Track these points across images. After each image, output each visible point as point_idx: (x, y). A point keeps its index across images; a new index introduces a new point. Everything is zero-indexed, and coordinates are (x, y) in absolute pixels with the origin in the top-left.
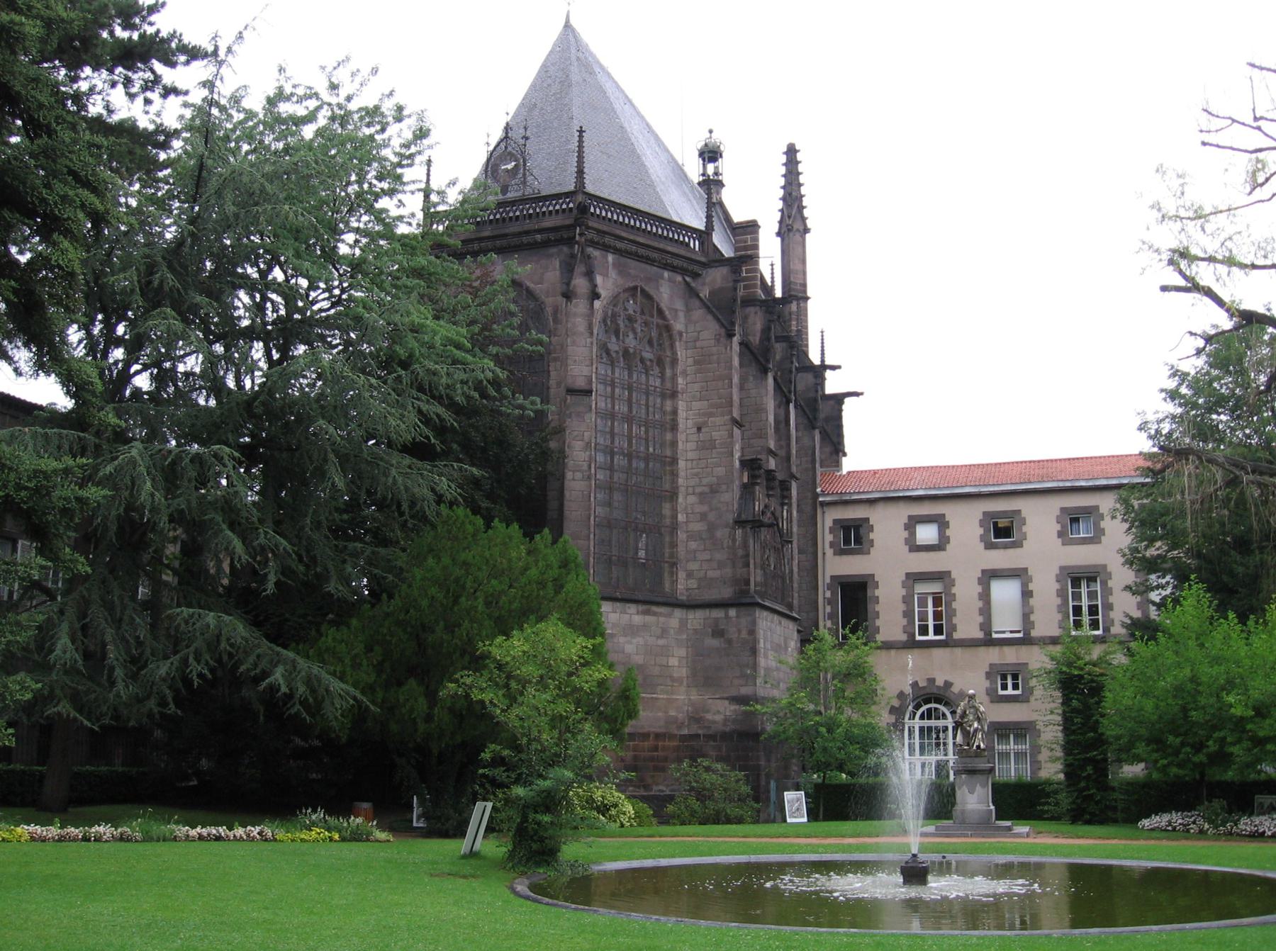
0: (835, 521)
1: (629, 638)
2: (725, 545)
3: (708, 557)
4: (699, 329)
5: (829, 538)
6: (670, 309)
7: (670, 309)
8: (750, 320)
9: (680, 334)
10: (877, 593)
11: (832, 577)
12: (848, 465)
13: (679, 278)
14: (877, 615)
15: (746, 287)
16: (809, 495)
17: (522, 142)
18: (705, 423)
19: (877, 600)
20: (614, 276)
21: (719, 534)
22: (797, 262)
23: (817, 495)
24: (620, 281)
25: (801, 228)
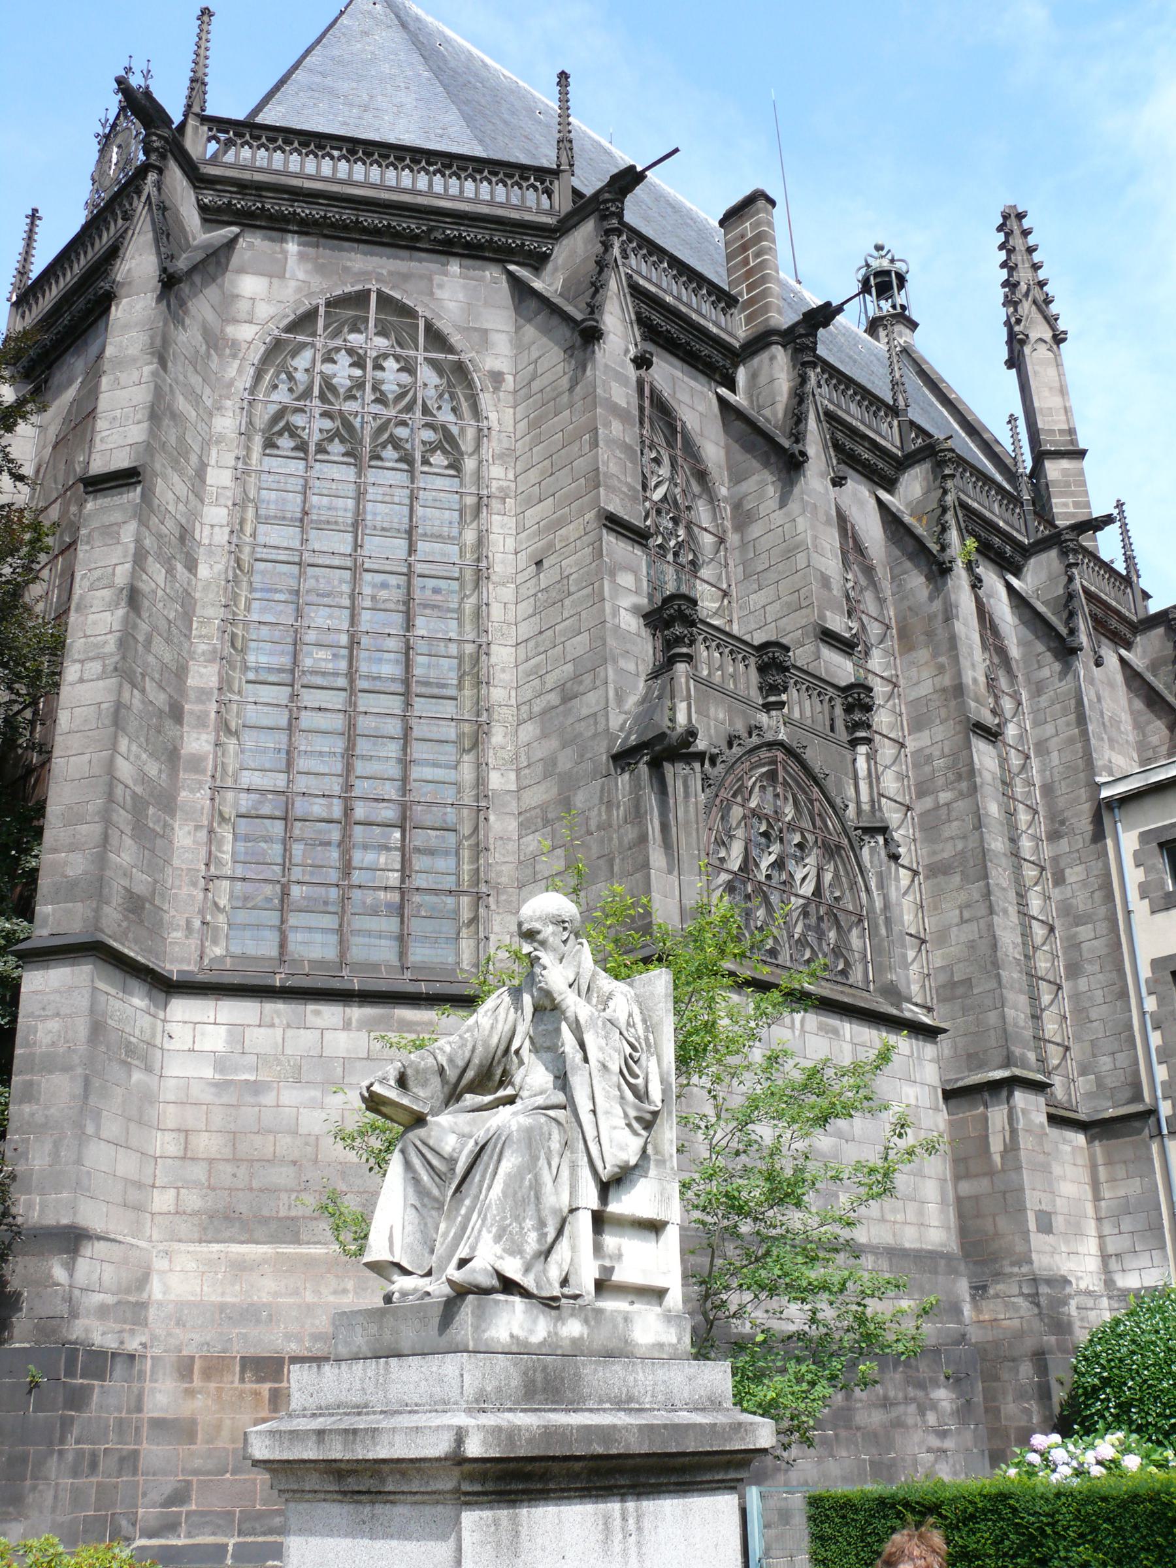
0: (1144, 837)
2: (593, 824)
5: (1134, 876)
6: (465, 330)
7: (465, 330)
8: (762, 379)
9: (497, 378)
11: (1156, 963)
15: (749, 319)
16: (1083, 793)
20: (301, 275)
22: (1046, 393)
24: (317, 283)
25: (1048, 335)
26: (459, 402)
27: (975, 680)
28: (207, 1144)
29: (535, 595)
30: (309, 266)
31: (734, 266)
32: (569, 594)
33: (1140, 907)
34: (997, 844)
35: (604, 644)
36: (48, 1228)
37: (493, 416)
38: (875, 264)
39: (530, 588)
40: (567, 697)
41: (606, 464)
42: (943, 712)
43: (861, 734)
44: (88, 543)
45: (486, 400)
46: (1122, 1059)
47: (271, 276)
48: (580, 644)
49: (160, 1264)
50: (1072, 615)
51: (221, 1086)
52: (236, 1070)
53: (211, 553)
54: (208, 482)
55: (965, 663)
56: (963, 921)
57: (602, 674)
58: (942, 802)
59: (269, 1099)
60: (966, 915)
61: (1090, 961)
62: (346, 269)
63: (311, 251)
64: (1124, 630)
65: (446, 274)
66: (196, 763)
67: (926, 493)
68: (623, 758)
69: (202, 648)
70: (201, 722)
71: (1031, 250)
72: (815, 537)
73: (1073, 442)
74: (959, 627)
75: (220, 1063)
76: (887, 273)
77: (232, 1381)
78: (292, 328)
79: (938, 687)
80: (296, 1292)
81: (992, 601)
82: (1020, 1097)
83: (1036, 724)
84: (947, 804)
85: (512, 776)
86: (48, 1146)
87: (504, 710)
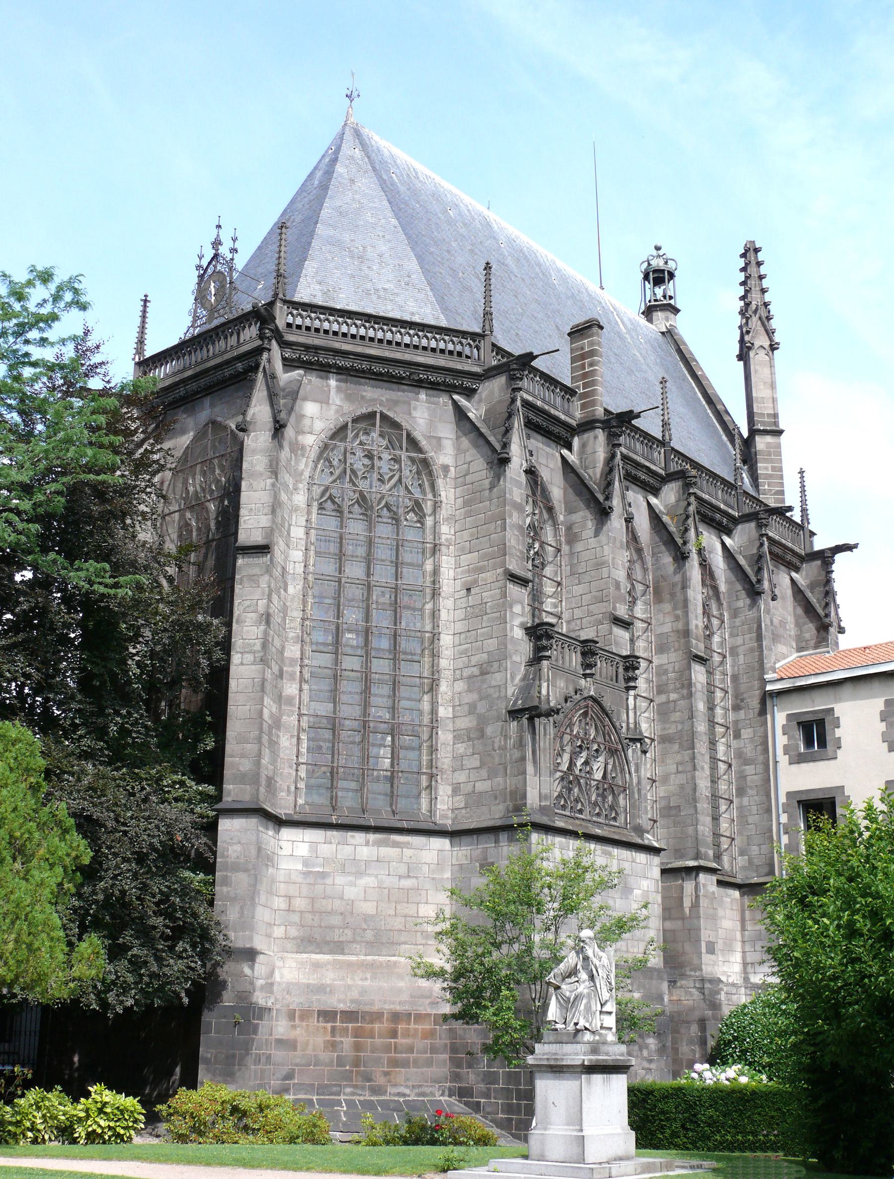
0: (790, 717)
2: (496, 746)
4: (469, 459)
5: (782, 740)
6: (429, 438)
7: (429, 438)
8: (589, 450)
9: (446, 469)
11: (789, 794)
12: (845, 642)
15: (583, 406)
16: (756, 684)
17: (229, 256)
18: (476, 581)
20: (338, 402)
21: (489, 731)
22: (762, 387)
23: (765, 682)
25: (766, 344)
26: (423, 481)
27: (697, 626)
28: (300, 903)
29: (466, 608)
30: (343, 396)
31: (576, 367)
32: (486, 614)
34: (701, 727)
35: (506, 648)
36: (239, 948)
37: (443, 494)
38: (654, 263)
39: (462, 603)
40: (484, 673)
41: (509, 541)
42: (676, 644)
43: (632, 684)
44: (241, 584)
45: (440, 482)
46: (765, 849)
47: (322, 403)
48: (492, 644)
49: (279, 963)
50: (760, 570)
51: (307, 874)
52: (313, 866)
53: (294, 579)
54: (292, 535)
55: (691, 616)
56: (678, 772)
57: (504, 665)
58: (671, 699)
59: (329, 881)
60: (680, 769)
61: (751, 788)
62: (363, 397)
63: (343, 385)
64: (795, 560)
65: (417, 400)
66: (290, 701)
67: (678, 501)
68: (514, 714)
69: (291, 635)
70: (292, 676)
71: (761, 277)
72: (614, 558)
73: (776, 424)
74: (690, 593)
75: (306, 863)
76: (663, 271)
77: (314, 1021)
78: (333, 437)
79: (674, 629)
80: (343, 979)
81: (712, 556)
82: (702, 877)
83: (732, 635)
84: (674, 701)
85: (451, 709)
86: (237, 909)
87: (447, 672)
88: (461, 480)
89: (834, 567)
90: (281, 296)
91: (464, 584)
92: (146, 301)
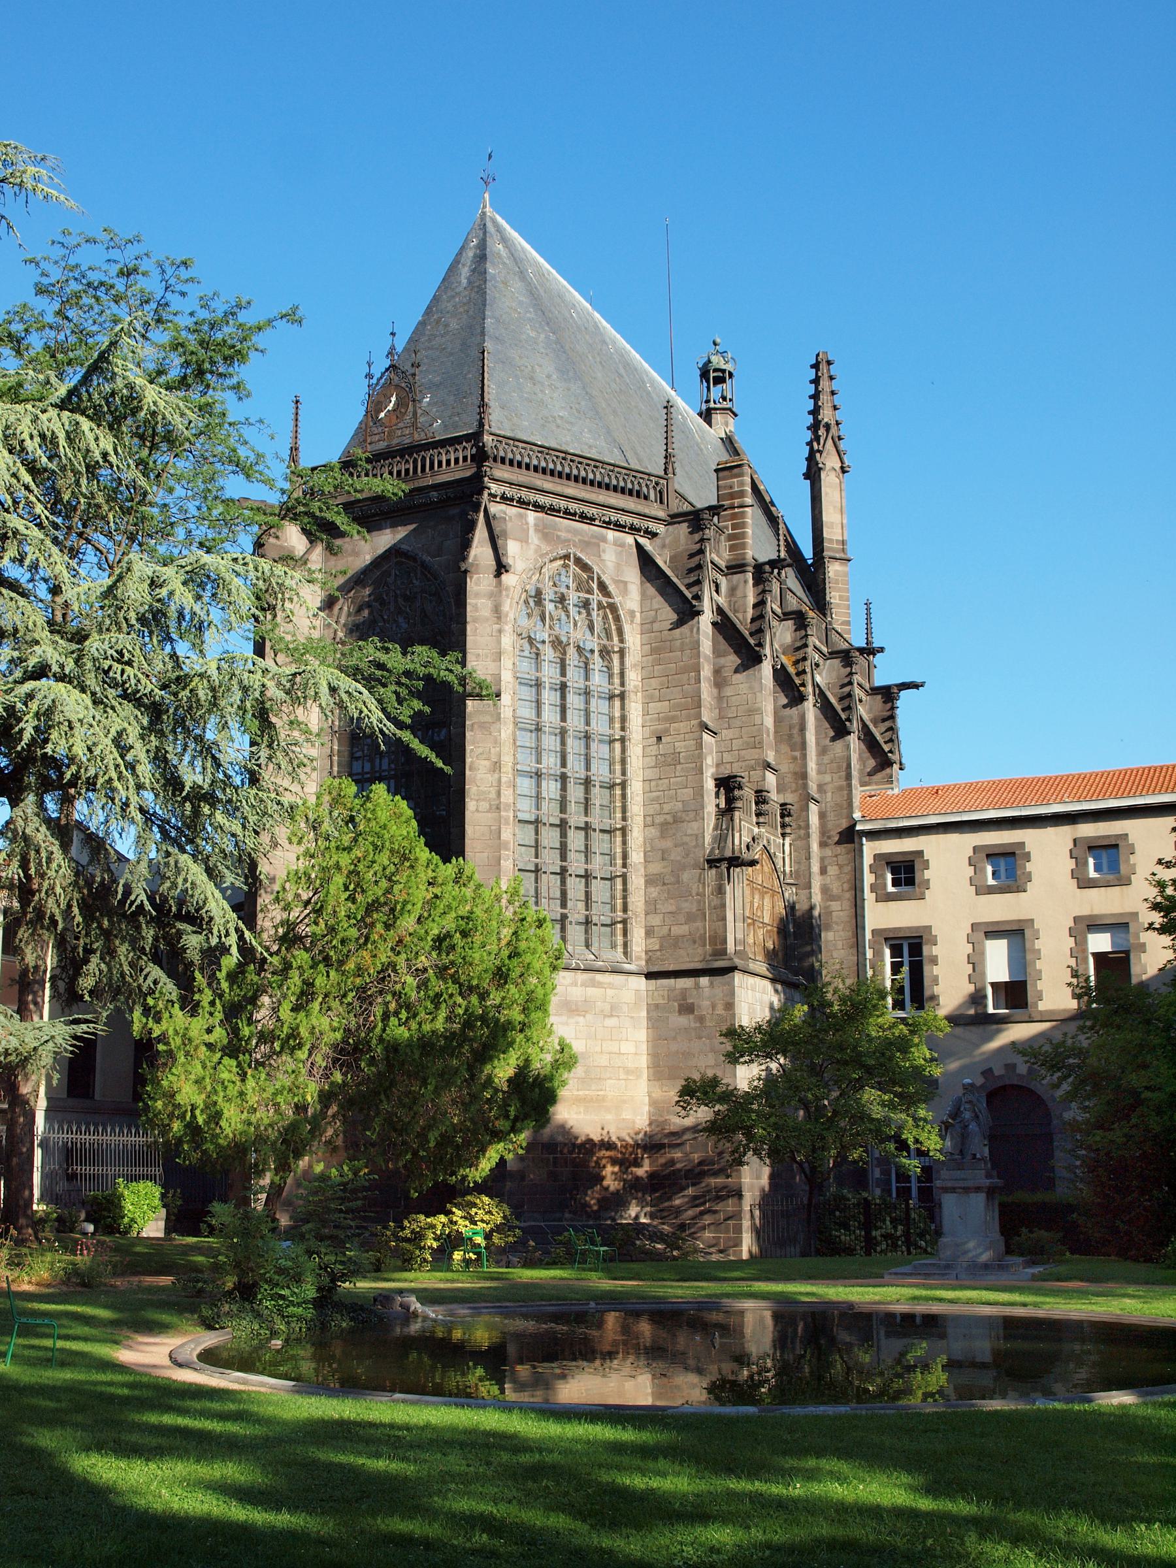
1: (564, 1018)
3: (672, 908)
4: (656, 606)
7: (617, 582)
8: (739, 593)
9: (632, 613)
10: (935, 950)
12: (905, 779)
13: (630, 539)
14: (936, 981)
15: (732, 548)
18: (667, 731)
19: (934, 961)
21: (686, 876)
22: (831, 510)
24: (545, 548)
25: (838, 465)
33: (869, 896)
42: (794, 785)
45: (627, 628)
61: (837, 924)
62: (558, 537)
68: (712, 863)
85: (642, 854)
88: (647, 627)
89: (898, 703)
90: (486, 427)
91: (652, 732)
92: (297, 402)
